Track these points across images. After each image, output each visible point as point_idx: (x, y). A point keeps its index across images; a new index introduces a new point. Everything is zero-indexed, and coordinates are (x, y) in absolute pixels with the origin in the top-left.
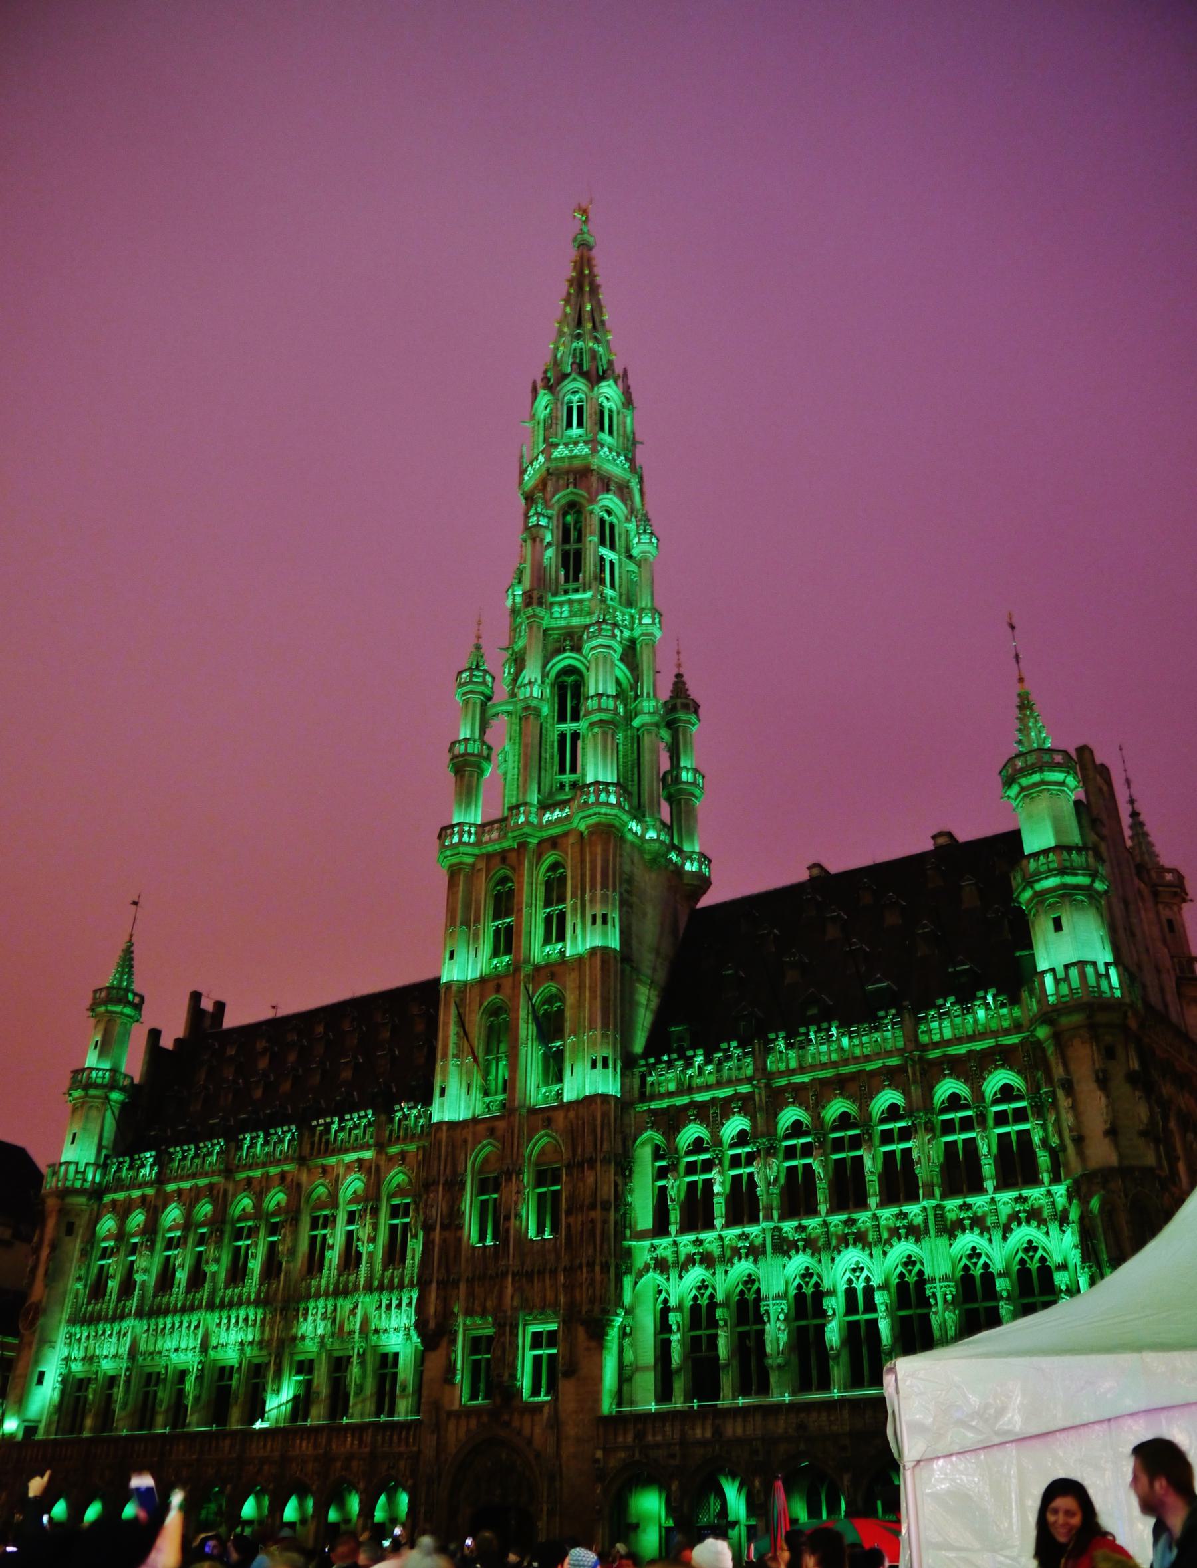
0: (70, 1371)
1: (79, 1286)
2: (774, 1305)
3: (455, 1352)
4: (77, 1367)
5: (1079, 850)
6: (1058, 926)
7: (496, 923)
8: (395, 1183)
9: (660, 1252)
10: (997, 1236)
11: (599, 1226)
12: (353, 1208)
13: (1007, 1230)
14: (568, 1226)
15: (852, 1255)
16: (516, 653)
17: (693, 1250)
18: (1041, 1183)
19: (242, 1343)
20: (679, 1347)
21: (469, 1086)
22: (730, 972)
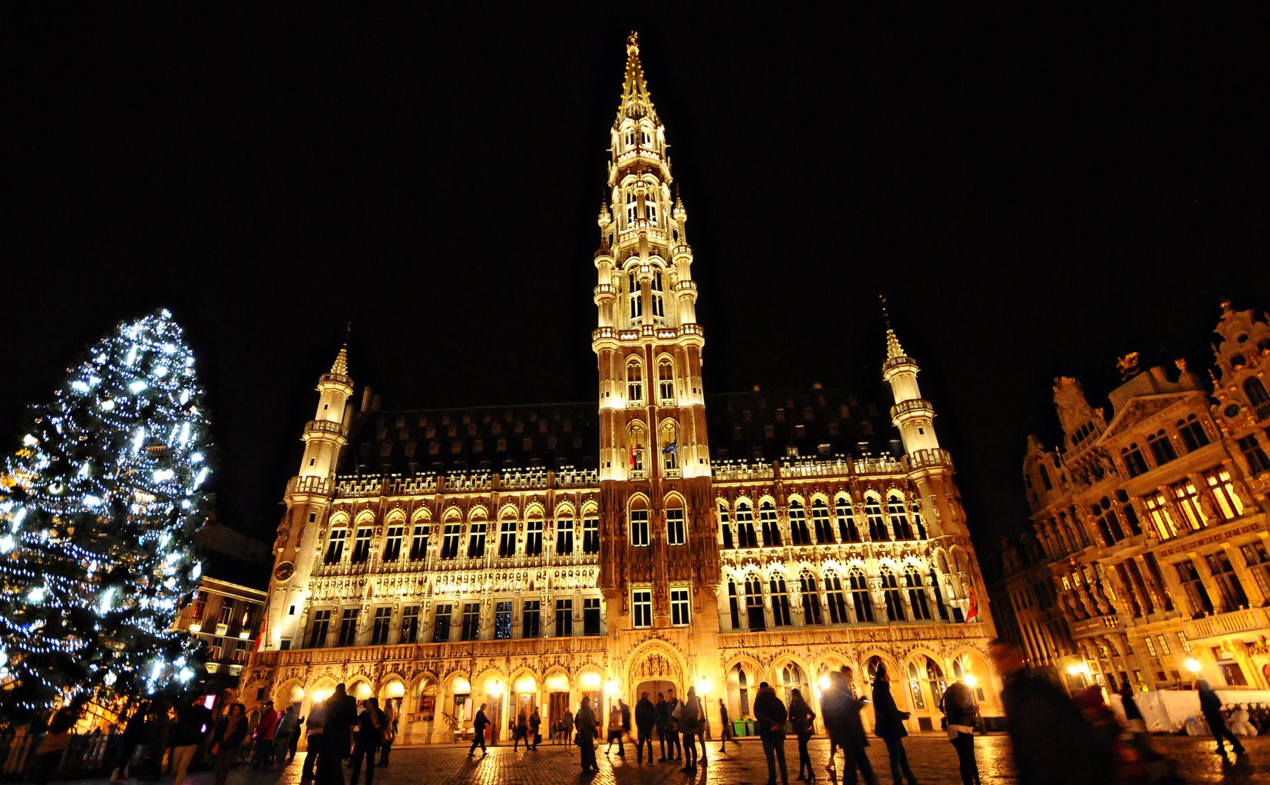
0: (312, 607)
1: (319, 553)
4: (319, 605)
5: (917, 400)
6: (921, 431)
8: (560, 510)
9: (728, 556)
10: (899, 559)
13: (902, 557)
14: (691, 539)
17: (748, 556)
19: (458, 592)
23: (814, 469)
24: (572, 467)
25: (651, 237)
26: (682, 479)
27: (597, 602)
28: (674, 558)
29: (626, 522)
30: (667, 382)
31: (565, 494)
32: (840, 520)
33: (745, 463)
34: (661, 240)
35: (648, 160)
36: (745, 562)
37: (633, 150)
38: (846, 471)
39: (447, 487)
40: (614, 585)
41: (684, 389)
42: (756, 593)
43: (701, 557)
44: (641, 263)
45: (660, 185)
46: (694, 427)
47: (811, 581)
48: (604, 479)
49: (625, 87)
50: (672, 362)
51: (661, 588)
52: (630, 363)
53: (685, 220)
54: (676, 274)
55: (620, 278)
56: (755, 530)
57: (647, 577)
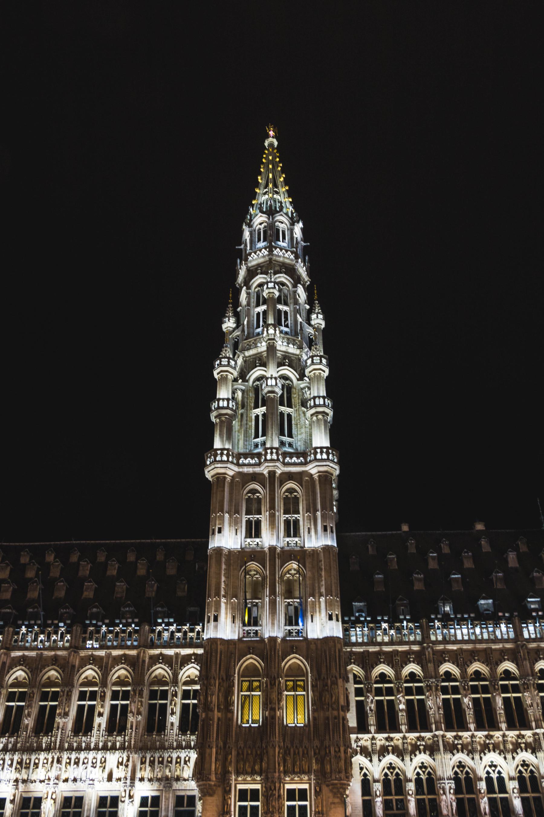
2: (448, 783)
3: (230, 798)
7: (248, 517)
8: (153, 675)
9: (362, 743)
11: (341, 721)
12: (115, 688)
14: (314, 719)
15: (492, 757)
16: (246, 357)
17: (387, 744)
18: (369, 732)
19: (16, 781)
20: (382, 806)
21: (234, 618)
22: (380, 576)
23: (471, 631)
24: (172, 620)
25: (281, 346)
26: (306, 639)
27: (191, 800)
28: (292, 742)
29: (233, 694)
30: (292, 517)
31: (161, 654)
32: (504, 699)
33: (385, 622)
34: (292, 350)
35: (281, 259)
36: (383, 751)
37: (265, 248)
38: (512, 635)
39: (16, 641)
40: (213, 777)
41: (312, 527)
42: (396, 795)
43: (327, 743)
44: (268, 375)
45: (295, 286)
46: (323, 573)
47: (468, 779)
48: (208, 637)
49: (260, 181)
50: (300, 492)
51: (274, 783)
52: (248, 492)
53: (323, 326)
54: (309, 388)
55: (243, 391)
56: (397, 709)
57: (257, 768)
